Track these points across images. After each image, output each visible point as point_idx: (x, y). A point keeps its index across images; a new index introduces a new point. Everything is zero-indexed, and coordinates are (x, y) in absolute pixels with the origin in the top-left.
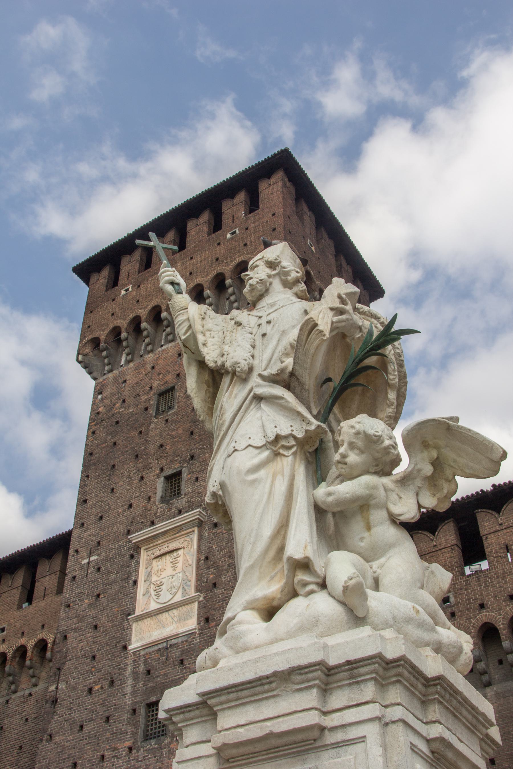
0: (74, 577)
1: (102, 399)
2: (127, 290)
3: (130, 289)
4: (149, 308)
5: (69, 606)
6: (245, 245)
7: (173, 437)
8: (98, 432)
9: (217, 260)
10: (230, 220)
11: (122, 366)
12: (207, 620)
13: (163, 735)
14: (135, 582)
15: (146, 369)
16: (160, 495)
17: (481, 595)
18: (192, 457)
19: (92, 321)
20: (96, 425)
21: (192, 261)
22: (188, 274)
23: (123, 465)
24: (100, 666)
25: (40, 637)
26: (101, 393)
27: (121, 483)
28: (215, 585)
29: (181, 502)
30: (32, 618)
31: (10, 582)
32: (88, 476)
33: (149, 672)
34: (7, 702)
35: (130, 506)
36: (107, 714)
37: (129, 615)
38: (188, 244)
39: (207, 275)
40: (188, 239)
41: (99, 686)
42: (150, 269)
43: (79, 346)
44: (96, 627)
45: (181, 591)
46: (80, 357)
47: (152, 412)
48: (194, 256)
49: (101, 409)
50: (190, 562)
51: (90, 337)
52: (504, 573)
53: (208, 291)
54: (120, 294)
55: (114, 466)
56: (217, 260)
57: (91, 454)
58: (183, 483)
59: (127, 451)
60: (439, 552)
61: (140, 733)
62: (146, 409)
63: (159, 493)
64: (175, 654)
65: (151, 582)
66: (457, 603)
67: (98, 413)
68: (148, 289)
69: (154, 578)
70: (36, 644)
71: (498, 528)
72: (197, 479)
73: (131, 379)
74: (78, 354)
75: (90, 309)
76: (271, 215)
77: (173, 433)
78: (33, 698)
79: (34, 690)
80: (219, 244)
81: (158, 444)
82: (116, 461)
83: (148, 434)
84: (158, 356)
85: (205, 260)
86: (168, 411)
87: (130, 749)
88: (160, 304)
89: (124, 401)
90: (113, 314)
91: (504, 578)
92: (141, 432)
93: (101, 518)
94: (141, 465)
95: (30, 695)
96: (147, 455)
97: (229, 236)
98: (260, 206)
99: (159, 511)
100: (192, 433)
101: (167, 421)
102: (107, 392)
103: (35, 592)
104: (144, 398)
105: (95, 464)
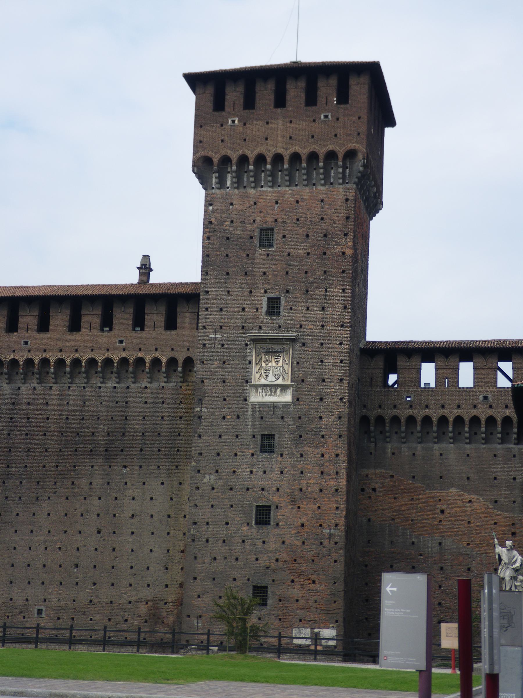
0: (204, 345)
1: (213, 211)
2: (233, 122)
3: (236, 122)
4: (256, 152)
5: (203, 362)
6: (336, 135)
7: (273, 270)
8: (212, 239)
9: (313, 137)
10: (324, 100)
11: (228, 188)
12: (298, 399)
13: (271, 452)
14: (250, 362)
15: (249, 202)
16: (266, 309)
17: (428, 400)
18: (288, 292)
19: (204, 138)
20: (209, 232)
21: (292, 125)
22: (288, 137)
23: (235, 275)
24: (229, 405)
25: (155, 356)
26: (211, 205)
27: (235, 289)
28: (303, 381)
29: (280, 320)
30: (146, 340)
31: (123, 308)
32: (207, 273)
33: (262, 418)
34: (128, 387)
35: (243, 309)
36: (237, 433)
37: (247, 382)
38: (287, 105)
39: (304, 148)
40: (288, 98)
41: (230, 417)
42: (254, 111)
43: (193, 158)
44: (224, 382)
45: (281, 377)
46: (195, 168)
47: (256, 241)
48: (294, 120)
49: (213, 220)
50: (287, 362)
51: (203, 154)
52: (442, 392)
53: (305, 165)
54: (228, 123)
55: (228, 274)
56: (313, 137)
57: (208, 256)
58: (281, 308)
59: (238, 266)
60: (410, 370)
61: (259, 448)
62: (251, 238)
63: (265, 308)
64: (279, 413)
65: (261, 367)
66: (414, 401)
67: (211, 222)
68: (254, 133)
69: (263, 364)
70: (151, 360)
71: (445, 367)
72: (291, 309)
73: (238, 206)
74: (194, 166)
75: (200, 122)
76: (357, 117)
77: (273, 267)
78: (149, 390)
79: (148, 385)
80: (314, 121)
81: (262, 270)
82: (230, 271)
83: (254, 259)
84: (259, 194)
85: (302, 130)
86: (269, 248)
87: (253, 455)
88: (265, 154)
89: (232, 222)
90: (222, 141)
91: (441, 395)
92: (248, 255)
93: (221, 309)
94: (249, 281)
95: (146, 387)
96: (253, 275)
97: (322, 117)
98: (349, 101)
99: (265, 320)
100: (287, 273)
101: (268, 255)
102: (218, 206)
103: (146, 323)
104: (249, 227)
105: (212, 265)
